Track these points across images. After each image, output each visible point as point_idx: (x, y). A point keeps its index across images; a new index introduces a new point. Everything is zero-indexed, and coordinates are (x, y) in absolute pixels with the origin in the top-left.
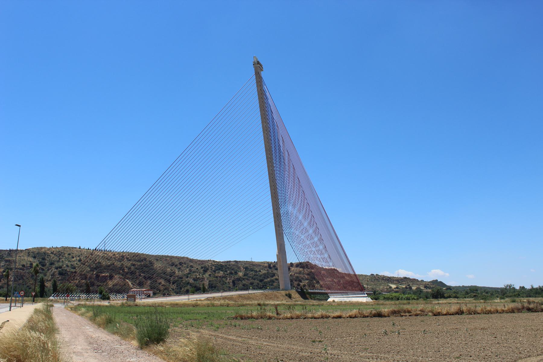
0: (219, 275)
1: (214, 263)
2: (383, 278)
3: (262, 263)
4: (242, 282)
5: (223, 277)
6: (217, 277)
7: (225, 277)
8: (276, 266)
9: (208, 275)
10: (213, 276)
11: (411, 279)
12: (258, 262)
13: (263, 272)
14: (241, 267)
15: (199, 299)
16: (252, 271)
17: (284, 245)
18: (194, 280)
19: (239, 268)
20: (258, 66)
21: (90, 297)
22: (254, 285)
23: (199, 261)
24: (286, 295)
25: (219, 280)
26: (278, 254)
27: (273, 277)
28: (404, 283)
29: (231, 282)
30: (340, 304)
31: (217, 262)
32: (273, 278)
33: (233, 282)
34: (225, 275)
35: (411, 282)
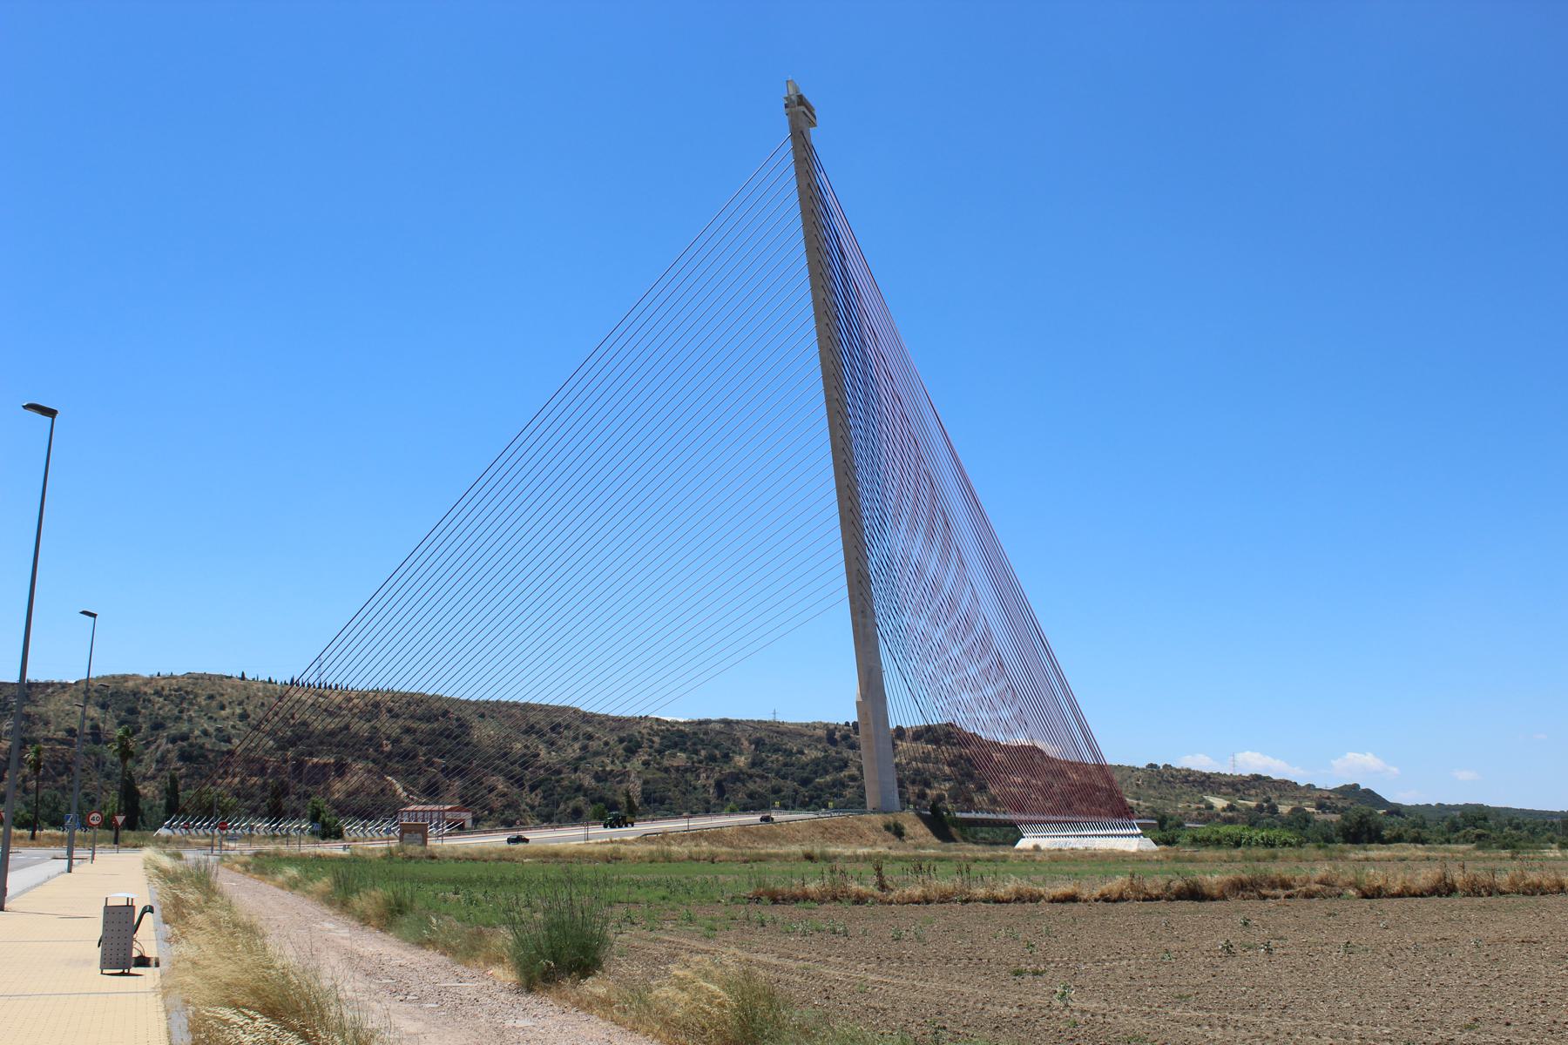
0: (675, 764)
1: (659, 725)
2: (1186, 777)
3: (807, 725)
4: (744, 785)
5: (686, 770)
6: (667, 770)
7: (693, 770)
8: (850, 737)
9: (640, 762)
10: (657, 766)
11: (1275, 781)
12: (796, 724)
13: (812, 754)
14: (743, 740)
15: (617, 839)
16: (776, 751)
17: (880, 672)
18: (598, 777)
19: (736, 742)
20: (800, 111)
21: (280, 830)
22: (783, 794)
23: (615, 719)
24: (887, 828)
25: (676, 779)
27: (841, 771)
28: (1253, 792)
29: (710, 785)
30: (1057, 857)
31: (667, 722)
32: (842, 775)
33: (719, 786)
34: (693, 763)
35: (1276, 789)
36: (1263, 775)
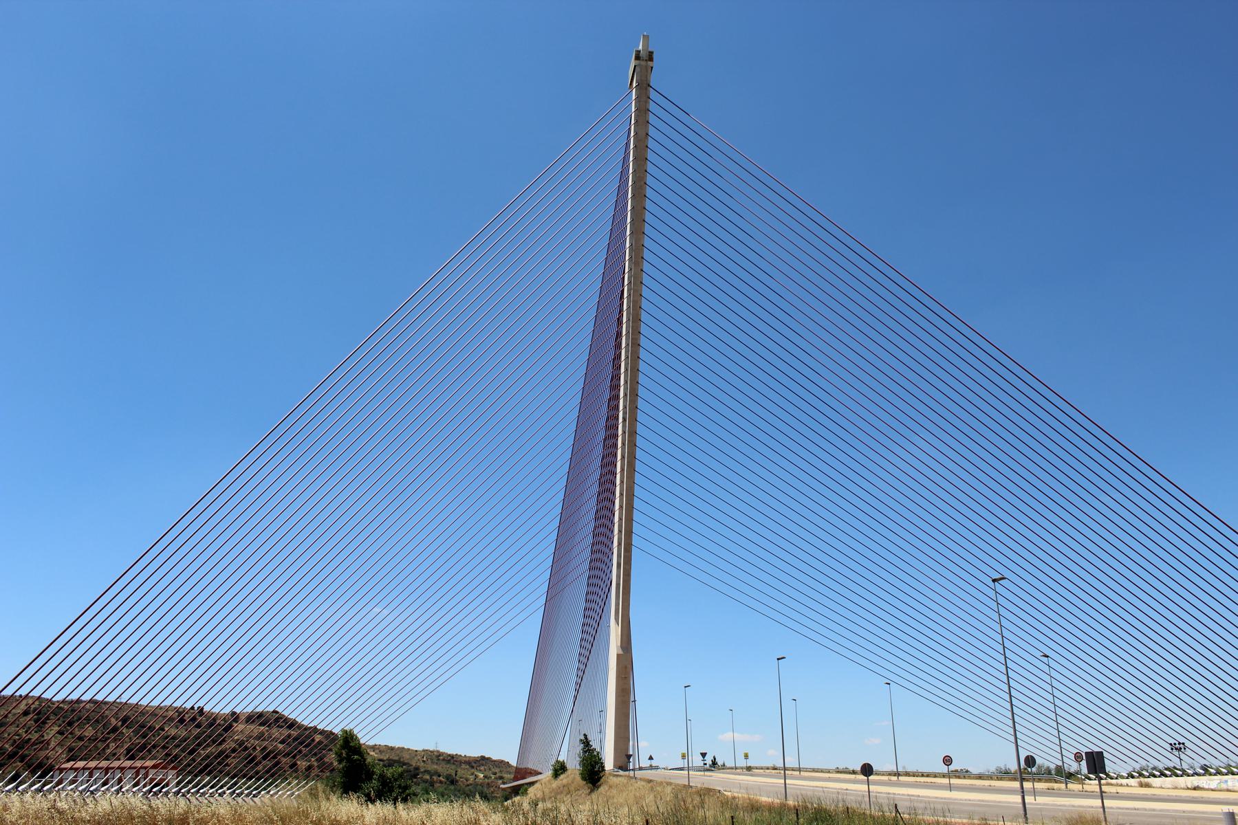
11: (495, 761)
26: (621, 652)
28: (482, 768)
35: (496, 766)
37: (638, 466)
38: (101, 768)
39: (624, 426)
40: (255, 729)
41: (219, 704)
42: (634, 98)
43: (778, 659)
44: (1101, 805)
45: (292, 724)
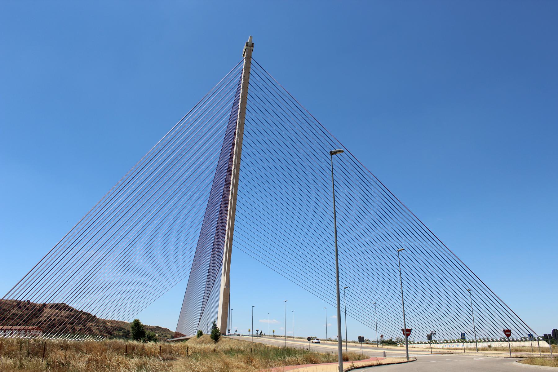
11: (163, 329)
26: (225, 288)
28: (157, 332)
36: (159, 326)
37: (237, 213)
38: (17, 329)
39: (232, 196)
40: (54, 311)
41: (37, 299)
42: (244, 62)
43: (285, 301)
44: (346, 349)
45: (71, 310)
